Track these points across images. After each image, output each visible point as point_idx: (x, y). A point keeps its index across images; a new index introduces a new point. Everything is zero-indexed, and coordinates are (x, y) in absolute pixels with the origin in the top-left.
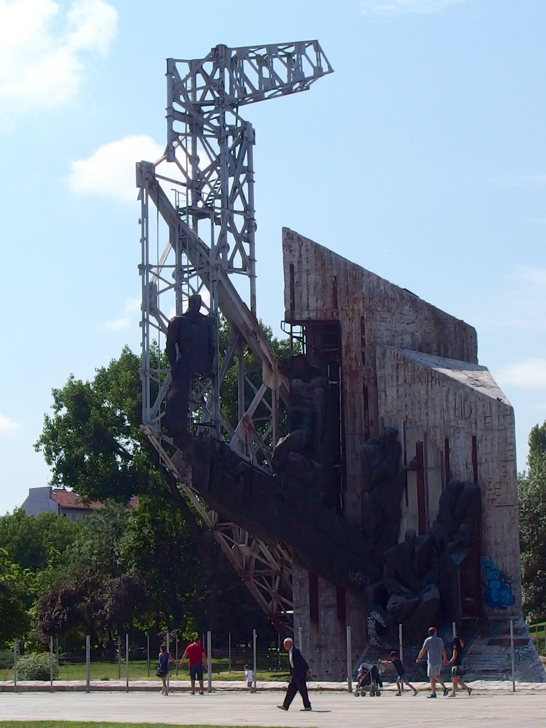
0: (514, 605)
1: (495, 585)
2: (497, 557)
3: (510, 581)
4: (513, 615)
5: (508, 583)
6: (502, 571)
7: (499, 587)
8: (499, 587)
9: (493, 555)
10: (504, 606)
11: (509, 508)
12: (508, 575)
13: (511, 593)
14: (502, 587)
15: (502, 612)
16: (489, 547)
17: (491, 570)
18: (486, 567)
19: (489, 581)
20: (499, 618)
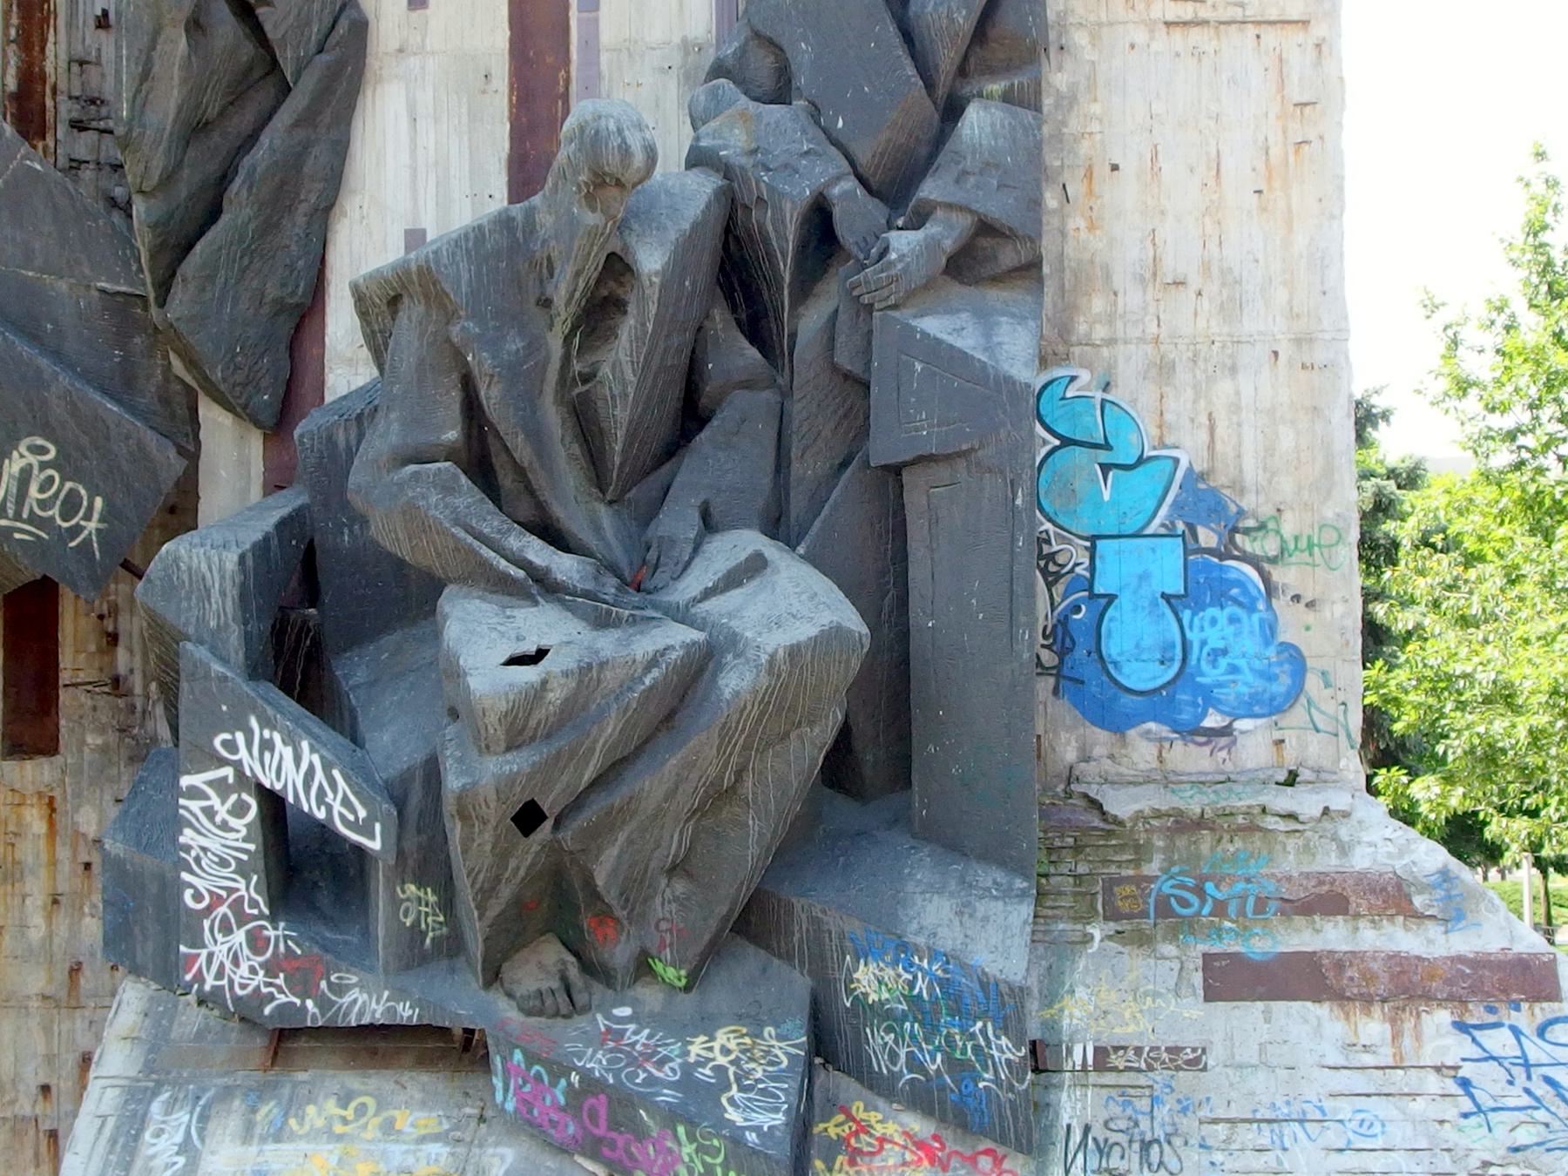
0: (1298, 715)
1: (1139, 572)
2: (1164, 370)
3: (1270, 546)
4: (1292, 780)
5: (1246, 558)
6: (1202, 477)
7: (1177, 587)
8: (1177, 587)
9: (1129, 364)
10: (1212, 720)
11: (1271, 37)
12: (1248, 503)
13: (1269, 630)
14: (1199, 590)
15: (1190, 758)
16: (1098, 304)
17: (1106, 468)
18: (1066, 442)
19: (1094, 539)
20: (1194, 803)
